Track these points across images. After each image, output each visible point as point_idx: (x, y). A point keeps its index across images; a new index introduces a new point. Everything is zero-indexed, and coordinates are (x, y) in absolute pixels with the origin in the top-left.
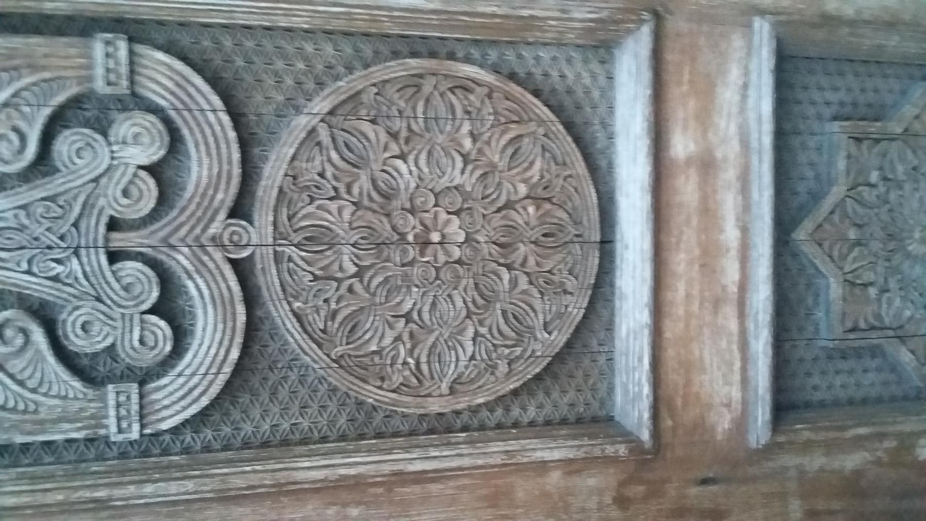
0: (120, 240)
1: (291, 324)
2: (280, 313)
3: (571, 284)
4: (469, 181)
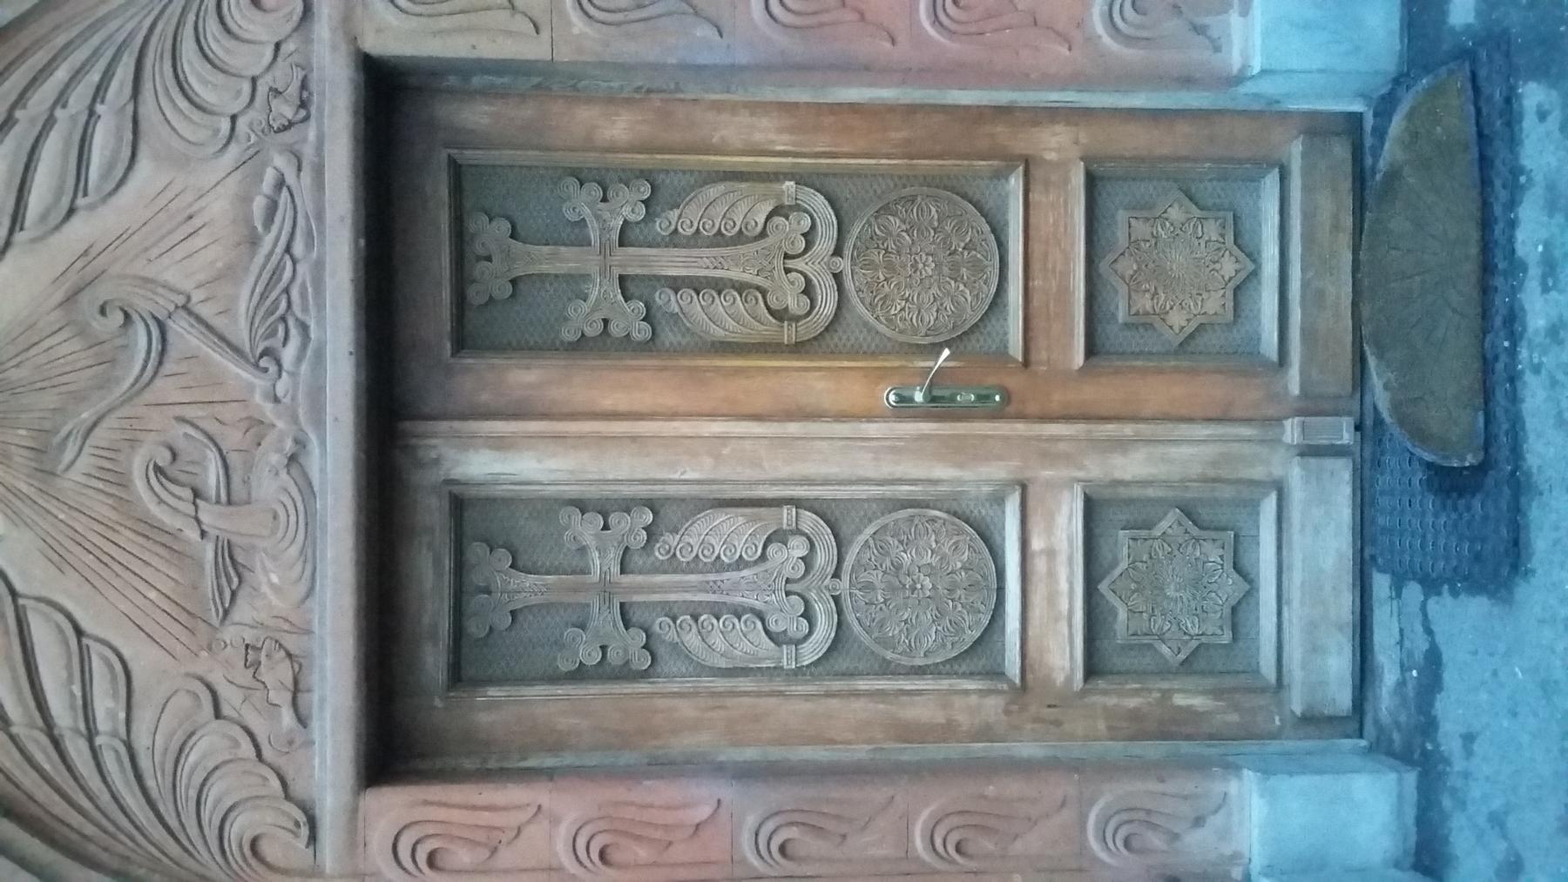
0: (790, 587)
1: (856, 623)
2: (851, 617)
3: (982, 608)
4: (934, 561)
